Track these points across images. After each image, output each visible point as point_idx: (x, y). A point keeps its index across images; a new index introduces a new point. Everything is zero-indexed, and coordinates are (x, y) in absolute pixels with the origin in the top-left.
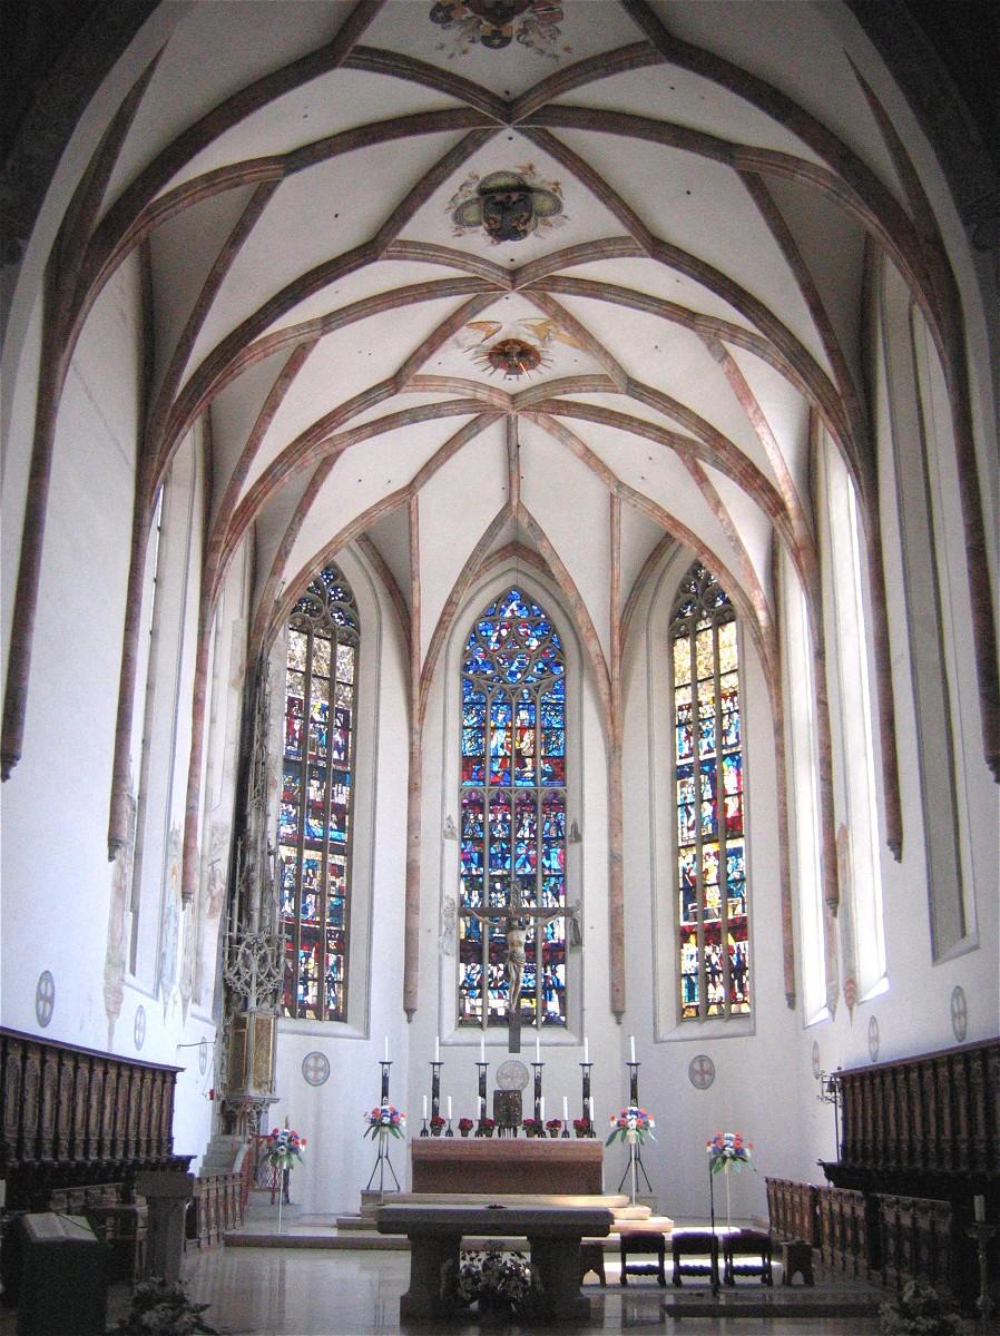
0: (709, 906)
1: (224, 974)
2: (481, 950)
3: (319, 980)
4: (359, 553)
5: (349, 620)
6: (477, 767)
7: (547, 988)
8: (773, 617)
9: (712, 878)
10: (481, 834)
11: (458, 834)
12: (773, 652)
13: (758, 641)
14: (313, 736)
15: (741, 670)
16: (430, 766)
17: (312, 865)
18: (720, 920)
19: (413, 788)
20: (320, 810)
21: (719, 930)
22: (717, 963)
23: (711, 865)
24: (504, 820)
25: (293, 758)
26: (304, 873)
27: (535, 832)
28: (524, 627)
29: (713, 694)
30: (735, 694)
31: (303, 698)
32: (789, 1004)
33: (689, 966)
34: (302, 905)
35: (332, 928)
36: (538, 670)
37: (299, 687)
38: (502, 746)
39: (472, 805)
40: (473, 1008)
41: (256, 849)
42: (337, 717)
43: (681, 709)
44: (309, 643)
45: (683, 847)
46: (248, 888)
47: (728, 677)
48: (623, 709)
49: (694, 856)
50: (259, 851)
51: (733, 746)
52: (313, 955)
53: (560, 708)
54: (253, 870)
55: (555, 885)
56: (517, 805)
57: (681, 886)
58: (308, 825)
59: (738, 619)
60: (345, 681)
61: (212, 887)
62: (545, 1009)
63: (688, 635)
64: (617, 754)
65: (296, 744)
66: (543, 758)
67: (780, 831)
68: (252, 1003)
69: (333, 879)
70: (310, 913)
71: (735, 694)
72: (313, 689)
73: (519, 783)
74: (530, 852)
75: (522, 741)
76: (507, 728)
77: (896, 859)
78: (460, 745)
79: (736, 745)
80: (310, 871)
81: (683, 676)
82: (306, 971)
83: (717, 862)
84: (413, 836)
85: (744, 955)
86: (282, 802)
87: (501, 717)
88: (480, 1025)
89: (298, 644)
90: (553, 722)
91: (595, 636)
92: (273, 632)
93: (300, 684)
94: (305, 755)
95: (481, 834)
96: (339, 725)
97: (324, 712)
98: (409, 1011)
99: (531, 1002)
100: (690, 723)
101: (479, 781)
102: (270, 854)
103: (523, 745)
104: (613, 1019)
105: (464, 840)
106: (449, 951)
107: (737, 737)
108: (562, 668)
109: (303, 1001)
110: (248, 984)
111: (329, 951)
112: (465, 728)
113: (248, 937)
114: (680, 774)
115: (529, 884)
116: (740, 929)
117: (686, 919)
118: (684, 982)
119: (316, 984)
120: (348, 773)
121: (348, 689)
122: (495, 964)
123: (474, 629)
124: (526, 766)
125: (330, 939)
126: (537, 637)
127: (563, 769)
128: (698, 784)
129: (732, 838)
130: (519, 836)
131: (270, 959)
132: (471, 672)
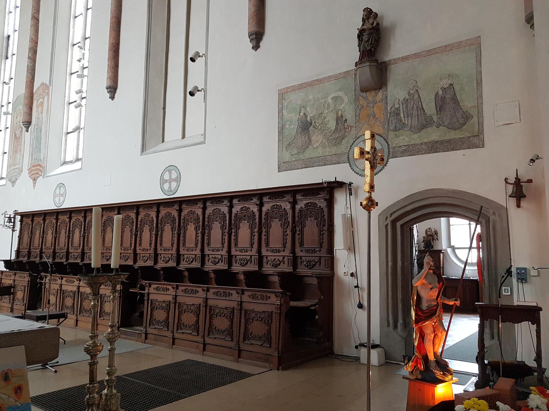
77: (110, 98)
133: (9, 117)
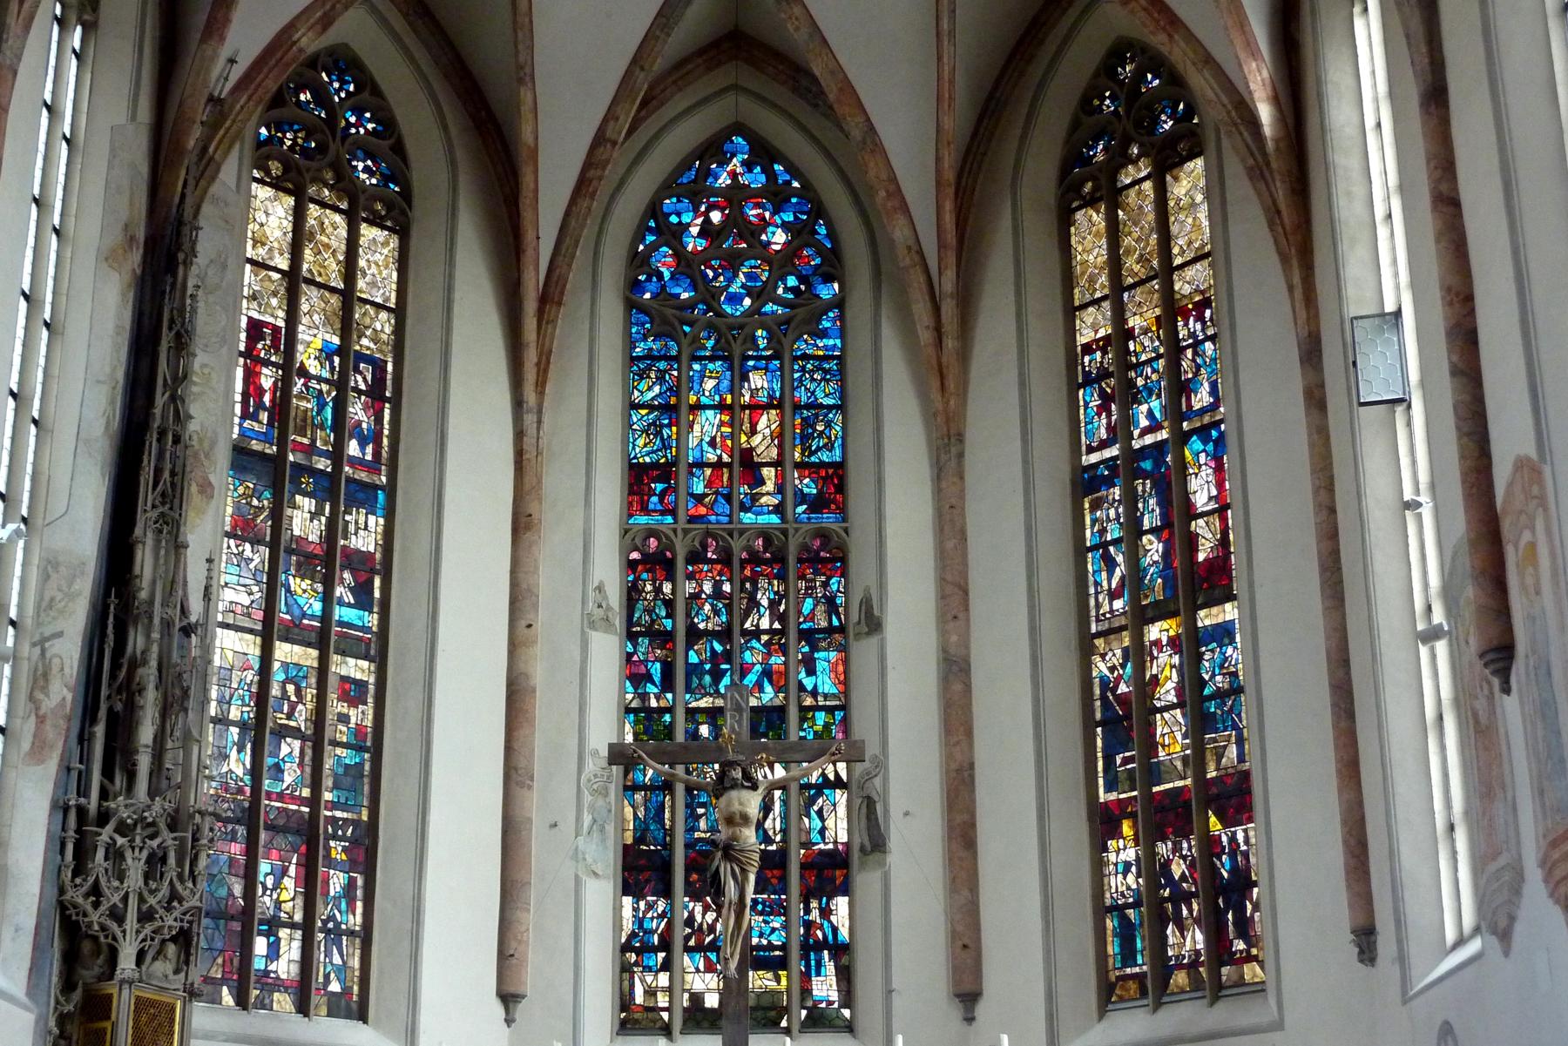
0: (1161, 753)
1: (62, 891)
2: (666, 868)
3: (307, 928)
4: (410, 40)
5: (386, 179)
6: (659, 487)
7: (811, 947)
8: (1290, 121)
9: (1167, 693)
10: (668, 623)
11: (618, 622)
12: (1293, 191)
13: (1259, 172)
14: (303, 404)
15: (1220, 256)
16: (559, 482)
17: (294, 676)
18: (1188, 782)
19: (522, 524)
20: (325, 561)
21: (1187, 805)
22: (1183, 877)
23: (1166, 666)
24: (717, 594)
25: (255, 445)
26: (275, 691)
27: (782, 618)
28: (757, 206)
29: (1158, 311)
30: (1206, 303)
31: (281, 323)
32: (1362, 952)
33: (1123, 885)
34: (269, 761)
35: (338, 814)
36: (787, 289)
37: (274, 302)
38: (712, 443)
39: (649, 561)
40: (651, 992)
41: (151, 618)
42: (357, 370)
43: (1088, 349)
44: (299, 215)
45: (1099, 635)
46: (132, 708)
47: (1189, 273)
48: (964, 356)
49: (1125, 651)
50: (157, 621)
51: (1203, 411)
52: (292, 870)
53: (837, 367)
54: (145, 662)
55: (827, 726)
56: (743, 563)
57: (1098, 716)
58: (288, 590)
59: (1211, 146)
60: (379, 300)
61: (39, 695)
62: (806, 991)
63: (1100, 199)
64: (954, 450)
65: (264, 417)
66: (798, 466)
67: (1323, 569)
68: (127, 963)
69: (342, 708)
70: (288, 779)
71: (1206, 303)
72: (305, 307)
73: (748, 518)
74: (773, 660)
75: (753, 432)
76: (721, 407)
78: (625, 442)
79: (1214, 407)
80: (291, 688)
81: (1092, 280)
82: (278, 904)
83: (1176, 660)
84: (523, 623)
85: (1246, 855)
86: (228, 535)
87: (709, 384)
88: (666, 1030)
89: (272, 214)
90: (819, 394)
91: (904, 208)
92: (207, 167)
93: (275, 294)
94: (282, 442)
95: (668, 623)
96: (363, 387)
97: (329, 357)
98: (508, 999)
99: (778, 981)
100: (1108, 375)
101: (663, 513)
102: (187, 631)
103: (756, 440)
104: (955, 1012)
105: (632, 637)
106: (599, 869)
107: (1214, 391)
108: (836, 286)
109: (266, 973)
110: (118, 916)
111: (331, 863)
112: (636, 406)
113: (121, 807)
114: (1087, 484)
115: (770, 726)
116: (1234, 797)
117: (1108, 789)
118: (1110, 924)
119: (298, 934)
120: (382, 488)
121: (384, 315)
122: (695, 896)
123: (654, 209)
124: (763, 483)
125: (334, 837)
126: (785, 226)
127: (841, 488)
128: (1131, 499)
129: (1208, 604)
130: (747, 625)
131: (172, 860)
132: (647, 296)
133: (1441, 647)
